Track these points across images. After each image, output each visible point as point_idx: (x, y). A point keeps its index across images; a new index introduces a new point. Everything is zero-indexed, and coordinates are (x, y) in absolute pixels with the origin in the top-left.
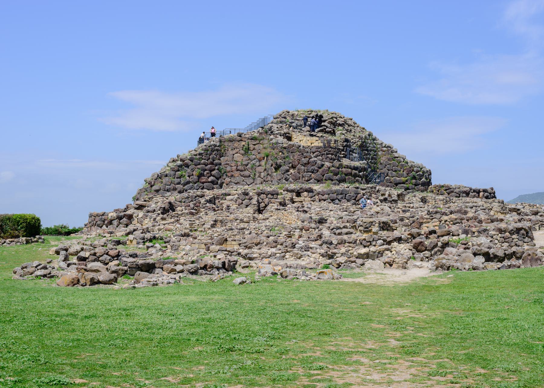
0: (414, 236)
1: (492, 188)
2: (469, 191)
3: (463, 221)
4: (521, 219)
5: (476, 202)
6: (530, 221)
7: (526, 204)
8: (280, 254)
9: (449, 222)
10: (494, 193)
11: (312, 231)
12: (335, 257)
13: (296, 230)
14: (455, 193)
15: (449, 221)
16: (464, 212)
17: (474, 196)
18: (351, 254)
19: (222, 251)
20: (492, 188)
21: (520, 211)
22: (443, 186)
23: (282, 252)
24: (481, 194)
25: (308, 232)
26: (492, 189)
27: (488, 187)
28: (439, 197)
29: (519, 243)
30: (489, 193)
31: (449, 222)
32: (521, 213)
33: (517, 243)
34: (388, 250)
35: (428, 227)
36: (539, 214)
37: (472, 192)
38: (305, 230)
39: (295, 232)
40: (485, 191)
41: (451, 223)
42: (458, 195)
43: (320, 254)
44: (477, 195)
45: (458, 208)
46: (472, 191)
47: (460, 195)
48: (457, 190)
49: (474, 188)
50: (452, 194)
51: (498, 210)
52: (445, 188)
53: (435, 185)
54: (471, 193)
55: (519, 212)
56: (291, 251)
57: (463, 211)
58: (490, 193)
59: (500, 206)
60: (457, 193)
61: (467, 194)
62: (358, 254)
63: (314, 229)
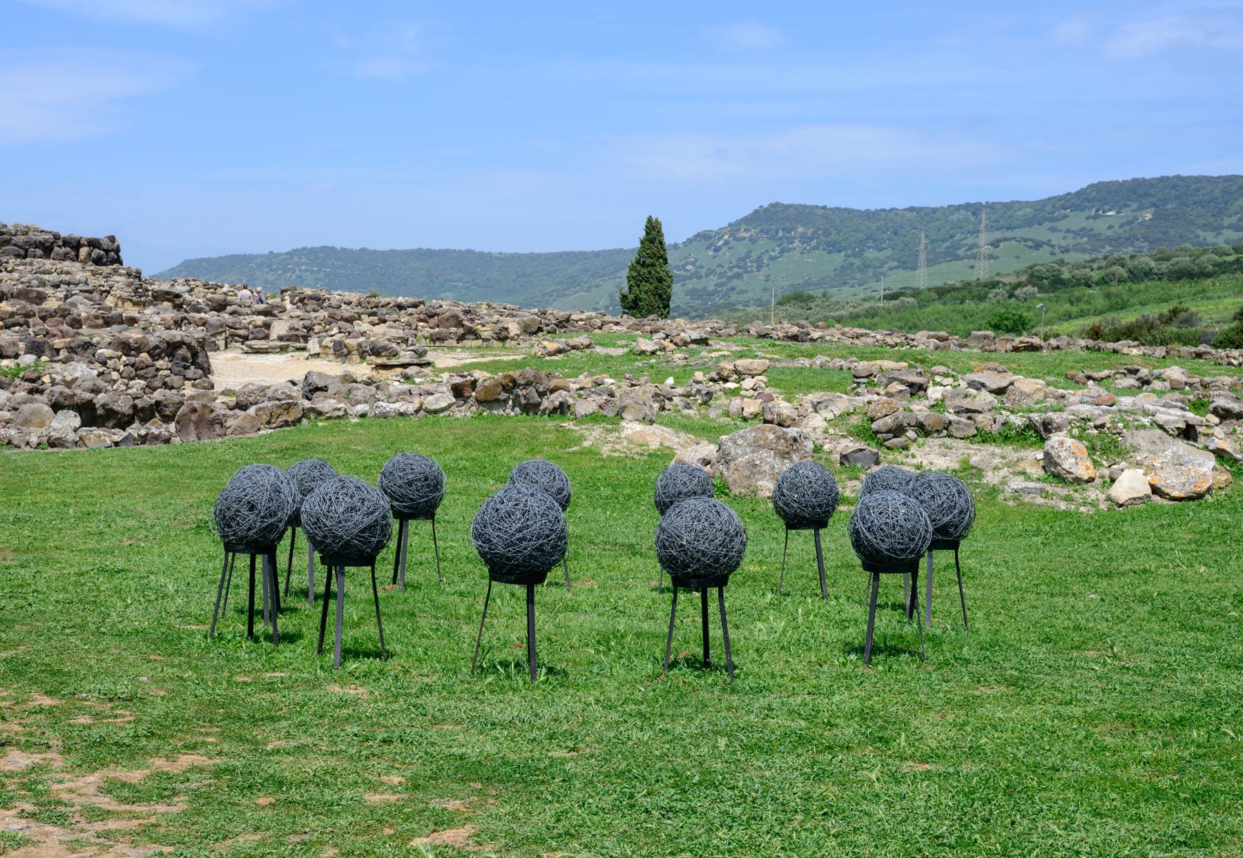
1: (113, 237)
2: (52, 244)
3: (31, 320)
4: (182, 321)
5: (68, 273)
6: (204, 325)
7: (198, 283)
10: (117, 250)
14: (15, 245)
16: (37, 297)
17: (65, 257)
20: (113, 237)
21: (181, 299)
24: (84, 251)
26: (112, 239)
27: (101, 234)
29: (172, 380)
30: (104, 250)
32: (182, 304)
33: (167, 379)
36: (229, 308)
37: (59, 246)
40: (93, 244)
42: (22, 252)
44: (73, 253)
45: (20, 286)
47: (26, 251)
48: (20, 239)
49: (64, 234)
50: (8, 247)
51: (125, 295)
54: (56, 249)
55: (178, 301)
57: (34, 295)
58: (107, 251)
59: (129, 285)
60: (20, 247)
61: (47, 249)
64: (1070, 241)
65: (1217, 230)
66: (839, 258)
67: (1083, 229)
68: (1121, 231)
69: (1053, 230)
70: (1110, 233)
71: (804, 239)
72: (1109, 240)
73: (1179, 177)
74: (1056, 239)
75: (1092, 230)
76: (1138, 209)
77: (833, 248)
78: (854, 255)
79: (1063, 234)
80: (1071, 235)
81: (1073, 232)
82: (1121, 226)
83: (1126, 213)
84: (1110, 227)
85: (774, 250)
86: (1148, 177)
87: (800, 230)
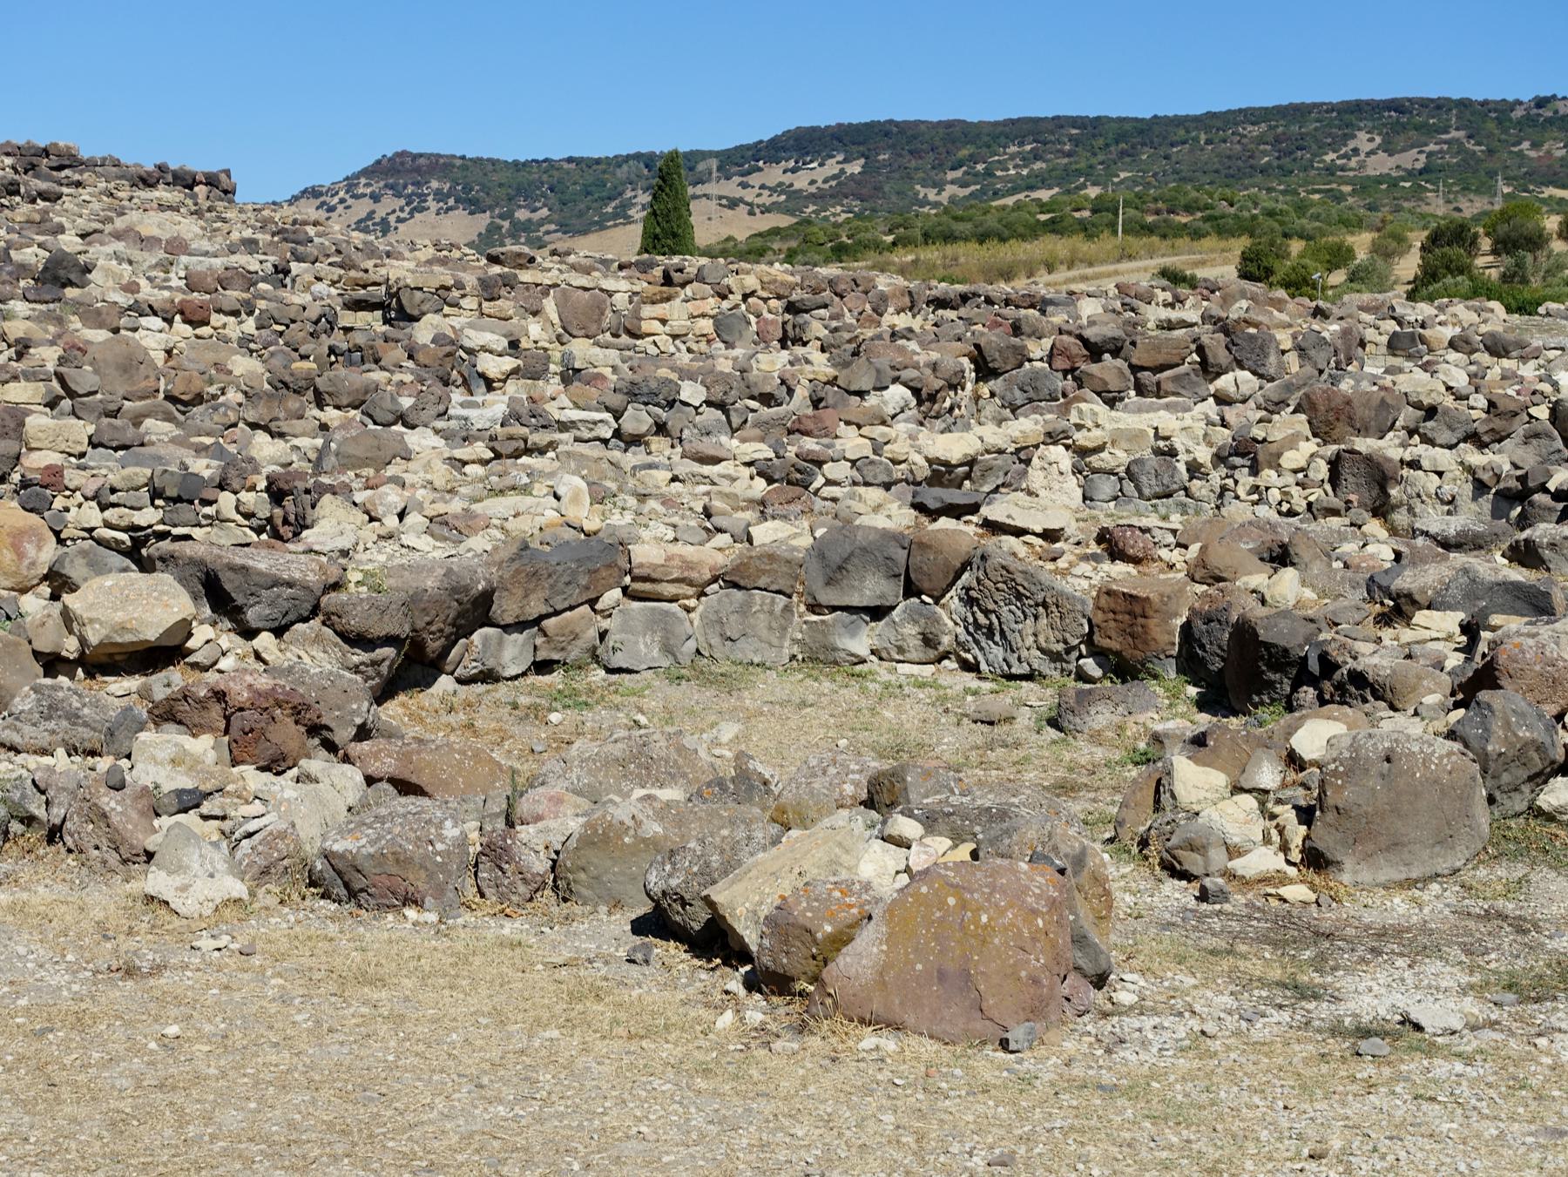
0: (996, 365)
8: (485, 463)
9: (765, 300)
11: (224, 326)
12: (819, 482)
13: (144, 321)
15: (765, 294)
18: (895, 462)
19: (116, 449)
22: (46, 152)
23: (498, 456)
25: (204, 331)
26: (227, 173)
27: (213, 168)
28: (156, 194)
31: (765, 300)
34: (1052, 438)
35: (664, 322)
38: (186, 321)
39: (135, 330)
41: (774, 303)
43: (749, 464)
46: (170, 179)
52: (54, 161)
53: (8, 143)
56: (552, 445)
62: (930, 461)
63: (232, 319)
64: (766, 199)
65: (939, 186)
66: (483, 220)
67: (780, 184)
68: (826, 186)
69: (744, 186)
70: (813, 189)
71: (440, 196)
72: (813, 198)
73: (891, 122)
74: (749, 195)
75: (791, 185)
76: (846, 161)
77: (475, 207)
78: (502, 217)
79: (757, 190)
80: (766, 193)
81: (770, 189)
82: (825, 181)
83: (832, 167)
84: (813, 182)
85: (402, 210)
86: (934, 117)
87: (435, 184)
